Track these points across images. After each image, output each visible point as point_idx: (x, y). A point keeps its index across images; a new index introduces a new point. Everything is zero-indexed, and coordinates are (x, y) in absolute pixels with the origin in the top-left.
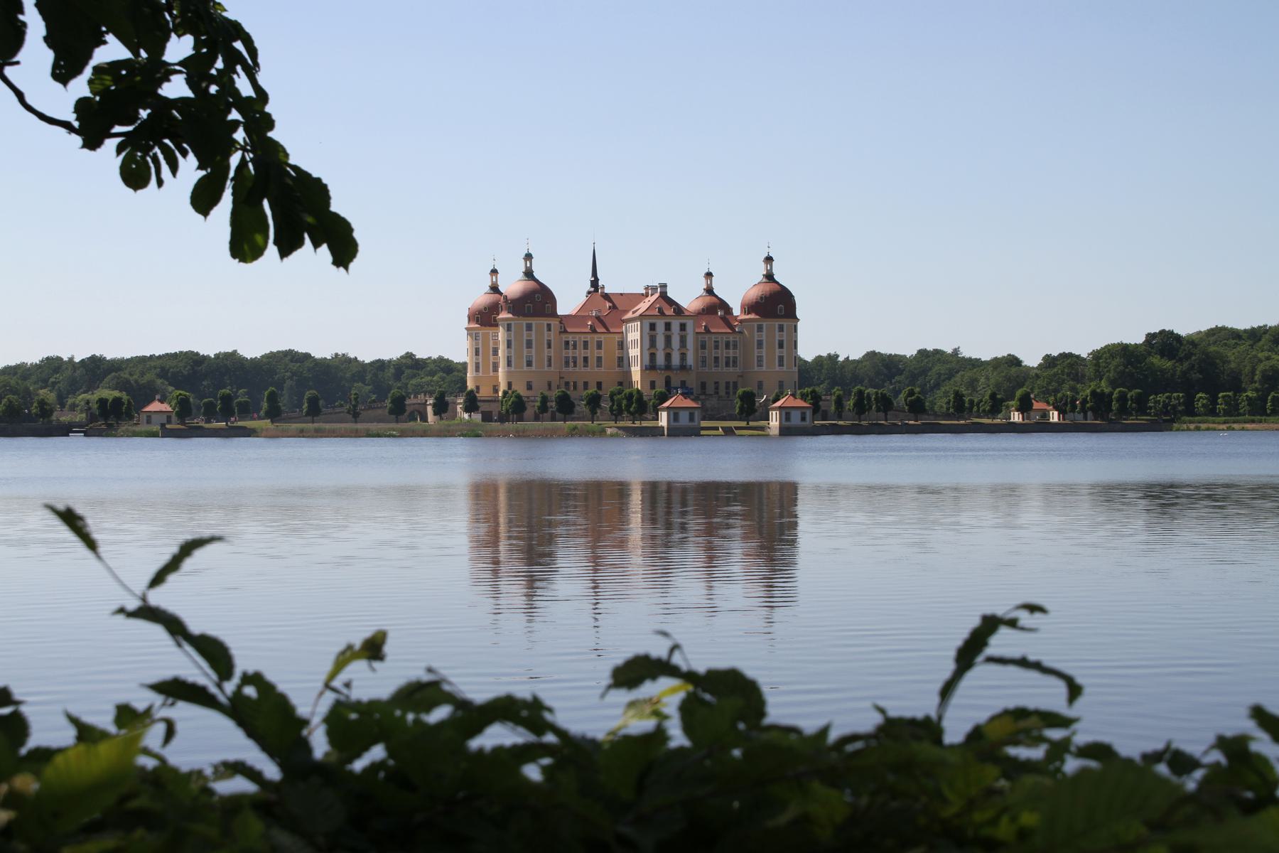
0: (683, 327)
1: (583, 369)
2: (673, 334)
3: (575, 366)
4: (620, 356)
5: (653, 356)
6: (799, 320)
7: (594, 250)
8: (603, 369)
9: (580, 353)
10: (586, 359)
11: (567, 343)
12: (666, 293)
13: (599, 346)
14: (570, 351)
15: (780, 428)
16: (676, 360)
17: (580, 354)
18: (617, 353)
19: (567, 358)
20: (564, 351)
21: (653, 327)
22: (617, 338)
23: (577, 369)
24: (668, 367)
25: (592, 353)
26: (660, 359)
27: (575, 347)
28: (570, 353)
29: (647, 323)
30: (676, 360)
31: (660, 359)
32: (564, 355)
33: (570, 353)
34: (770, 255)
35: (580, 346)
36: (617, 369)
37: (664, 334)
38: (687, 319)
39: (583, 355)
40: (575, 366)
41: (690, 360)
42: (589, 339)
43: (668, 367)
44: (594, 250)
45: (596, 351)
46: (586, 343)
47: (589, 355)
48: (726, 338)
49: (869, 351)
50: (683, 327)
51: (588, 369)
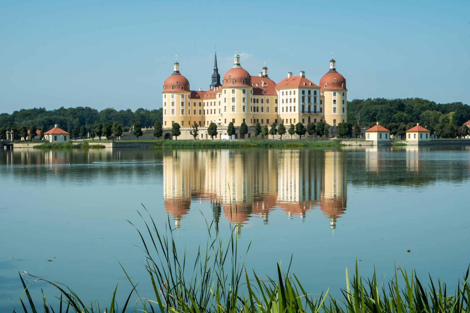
0: (315, 93)
1: (261, 113)
2: (311, 96)
3: (262, 111)
4: (182, 109)
5: (303, 106)
6: (347, 90)
7: (216, 55)
8: (269, 113)
9: (260, 105)
10: (262, 108)
11: (254, 100)
12: (305, 76)
13: (268, 101)
14: (256, 104)
15: (418, 141)
16: (312, 109)
17: (260, 105)
18: (275, 105)
19: (254, 107)
20: (261, 104)
21: (303, 92)
22: (275, 98)
23: (259, 113)
24: (309, 112)
25: (265, 105)
26: (306, 109)
27: (258, 102)
28: (256, 105)
29: (301, 90)
30: (312, 109)
31: (306, 109)
32: (266, 106)
33: (256, 105)
34: (334, 59)
35: (260, 101)
36: (275, 113)
37: (308, 96)
38: (317, 89)
39: (261, 106)
40: (262, 111)
41: (318, 110)
42: (263, 98)
43: (309, 112)
44: (216, 55)
45: (264, 106)
46: (262, 100)
47: (194, 107)
48: (194, 101)
49: (139, 108)
50: (315, 93)
51: (263, 113)
